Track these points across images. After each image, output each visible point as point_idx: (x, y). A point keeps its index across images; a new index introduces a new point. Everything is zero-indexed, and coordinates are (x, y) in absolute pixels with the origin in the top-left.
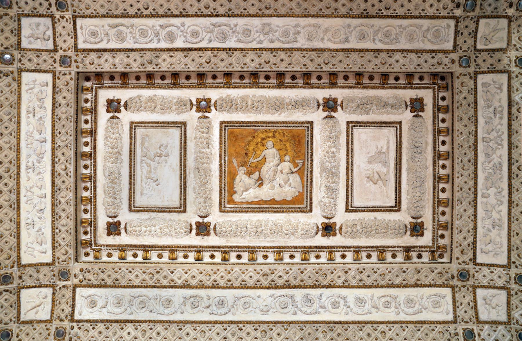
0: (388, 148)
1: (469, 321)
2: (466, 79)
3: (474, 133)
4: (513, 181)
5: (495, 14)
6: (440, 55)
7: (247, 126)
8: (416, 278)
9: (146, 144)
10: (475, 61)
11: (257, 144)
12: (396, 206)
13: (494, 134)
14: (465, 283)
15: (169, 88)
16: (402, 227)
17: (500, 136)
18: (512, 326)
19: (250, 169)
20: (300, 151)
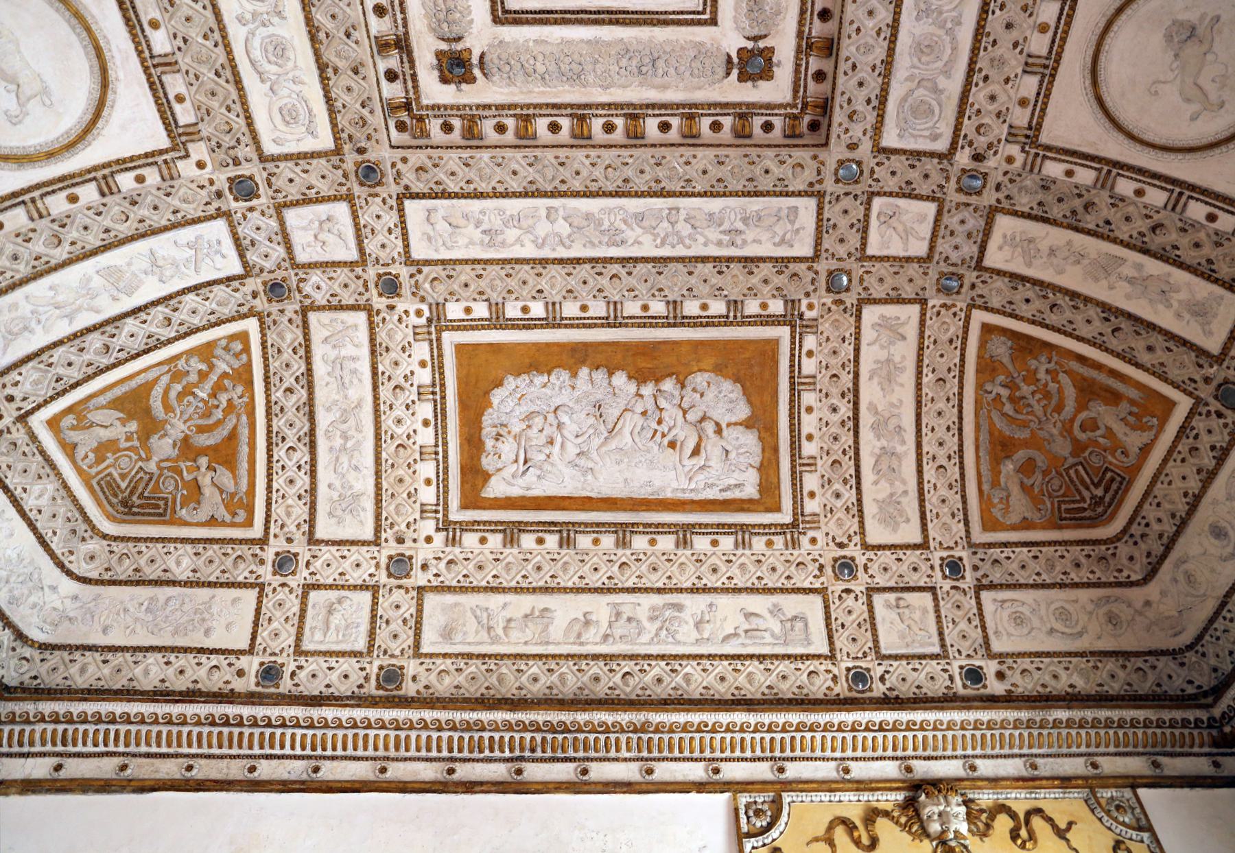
1: (274, 188)
2: (809, 174)
3: (689, 189)
4: (588, 266)
5: (942, 232)
6: (871, 118)
8: (341, 64)
10: (847, 194)
12: (506, 12)
13: (685, 230)
14: (352, 177)
16: (456, 30)
17: (681, 241)
18: (293, 273)
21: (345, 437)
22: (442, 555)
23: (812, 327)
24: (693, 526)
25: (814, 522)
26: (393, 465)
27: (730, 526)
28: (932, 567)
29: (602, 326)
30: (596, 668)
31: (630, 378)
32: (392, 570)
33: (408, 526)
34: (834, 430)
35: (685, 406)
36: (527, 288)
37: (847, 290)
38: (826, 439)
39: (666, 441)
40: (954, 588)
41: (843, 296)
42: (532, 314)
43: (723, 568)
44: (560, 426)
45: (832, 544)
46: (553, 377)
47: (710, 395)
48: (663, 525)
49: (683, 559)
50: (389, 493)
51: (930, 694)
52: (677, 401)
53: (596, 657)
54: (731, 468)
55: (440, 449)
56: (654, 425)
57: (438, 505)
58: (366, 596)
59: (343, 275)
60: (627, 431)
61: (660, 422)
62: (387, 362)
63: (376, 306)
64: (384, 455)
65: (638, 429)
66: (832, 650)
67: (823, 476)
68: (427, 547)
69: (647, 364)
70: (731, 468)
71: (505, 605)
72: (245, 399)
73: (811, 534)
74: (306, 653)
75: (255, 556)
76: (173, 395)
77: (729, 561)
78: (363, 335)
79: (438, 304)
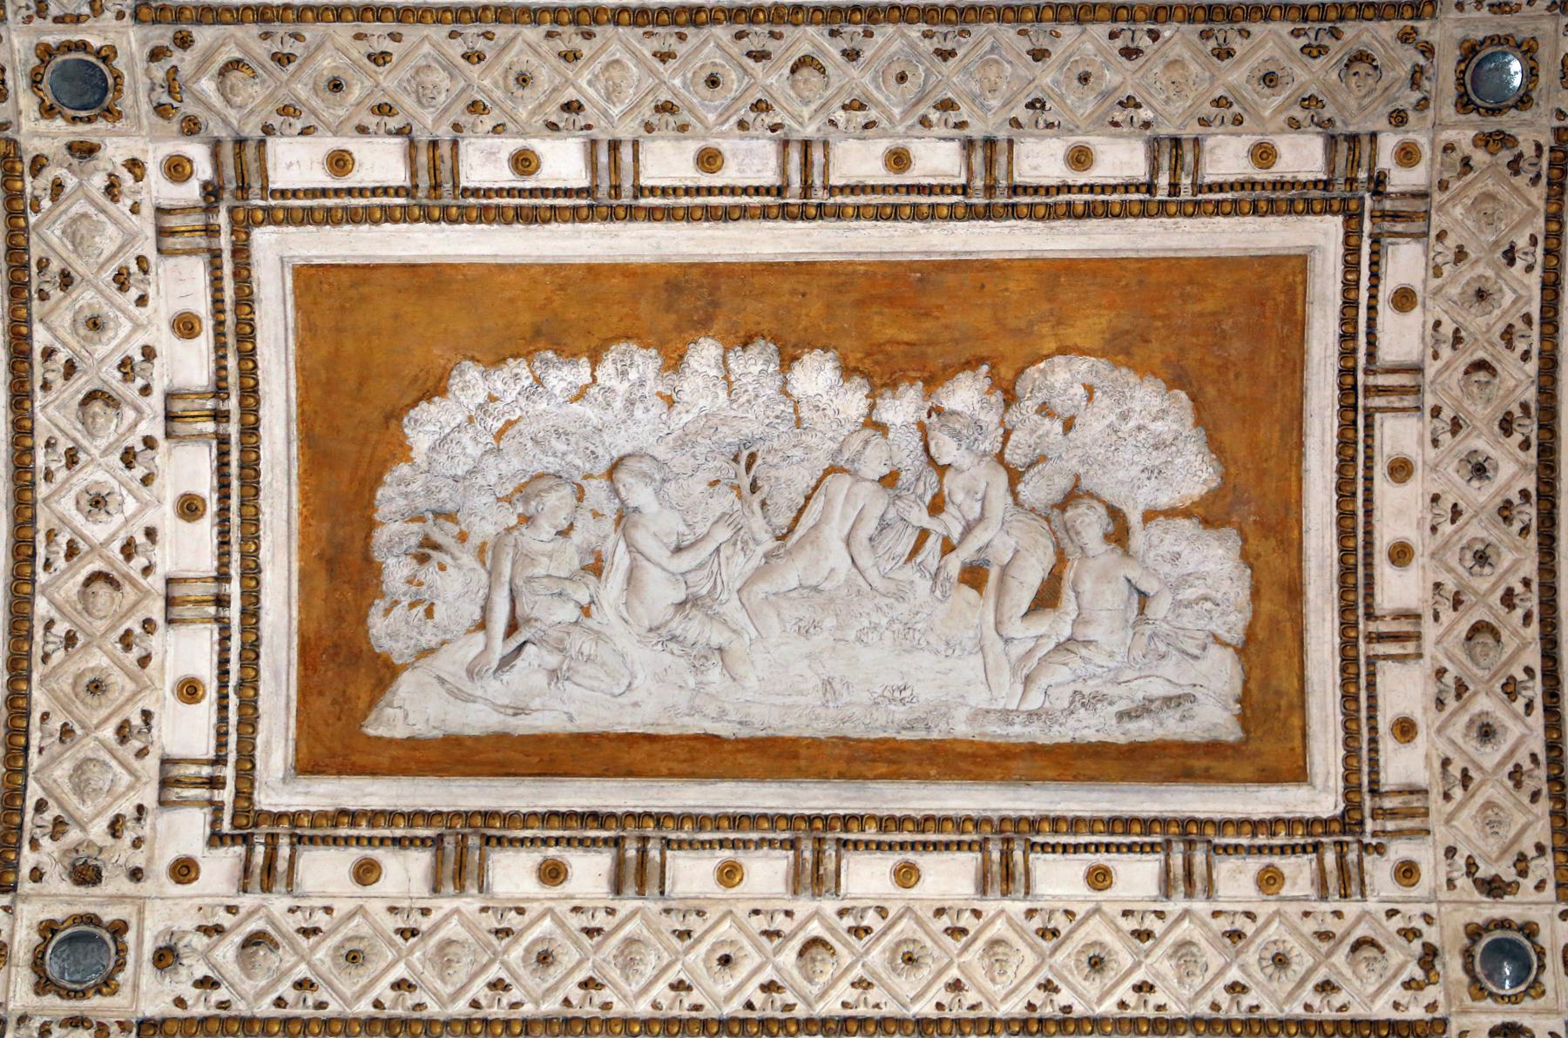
4: (723, 33)
22: (226, 920)
23: (1412, 215)
24: (1034, 824)
25: (1411, 814)
26: (70, 640)
27: (1147, 825)
29: (764, 214)
32: (52, 969)
34: (1476, 530)
35: (1015, 457)
36: (530, 98)
37: (1524, 101)
38: (1452, 559)
41: (1508, 121)
42: (547, 177)
43: (1122, 954)
44: (625, 517)
45: (1463, 882)
47: (1093, 425)
48: (939, 822)
49: (999, 928)
50: (55, 724)
55: (234, 589)
57: (219, 761)
60: (834, 534)
62: (63, 320)
63: (32, 146)
65: (870, 526)
67: (1440, 673)
69: (897, 328)
73: (1399, 850)
77: (1143, 935)
79: (240, 142)
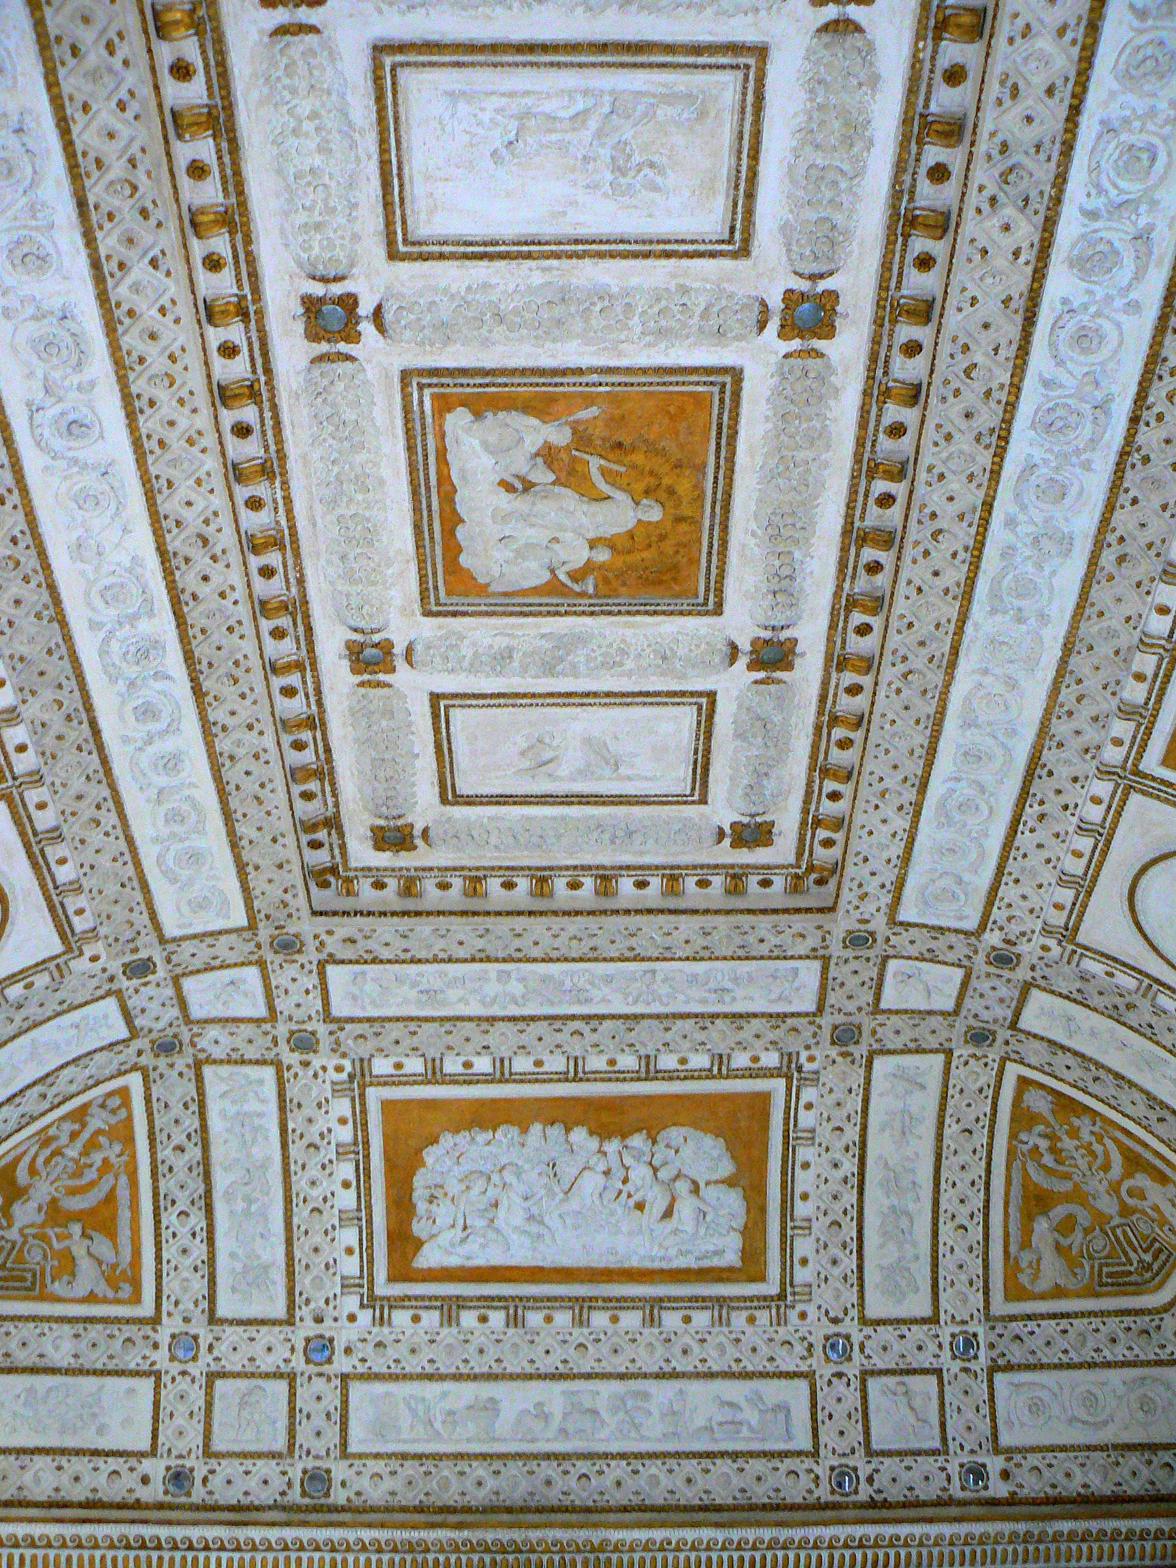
0: (629, 778)
7: (718, 445)
9: (670, 111)
11: (651, 473)
15: (896, 195)
19: (563, 455)
20: (624, 584)
21: (249, 1201)
24: (661, 1300)
27: (704, 1299)
28: (940, 1346)
30: (548, 1469)
31: (591, 1133)
33: (327, 1302)
39: (631, 1202)
40: (966, 1370)
42: (476, 1069)
46: (499, 1133)
48: (625, 1299)
51: (922, 1497)
52: (647, 1158)
53: (548, 1456)
54: (709, 1231)
56: (620, 1185)
58: (282, 1386)
59: (246, 1030)
61: (625, 1181)
64: (296, 1221)
66: (816, 1445)
68: (351, 1327)
70: (709, 1231)
71: (445, 1395)
72: (125, 1158)
73: (800, 1307)
74: (219, 1455)
75: (146, 1338)
76: (40, 1160)
78: (270, 1090)
